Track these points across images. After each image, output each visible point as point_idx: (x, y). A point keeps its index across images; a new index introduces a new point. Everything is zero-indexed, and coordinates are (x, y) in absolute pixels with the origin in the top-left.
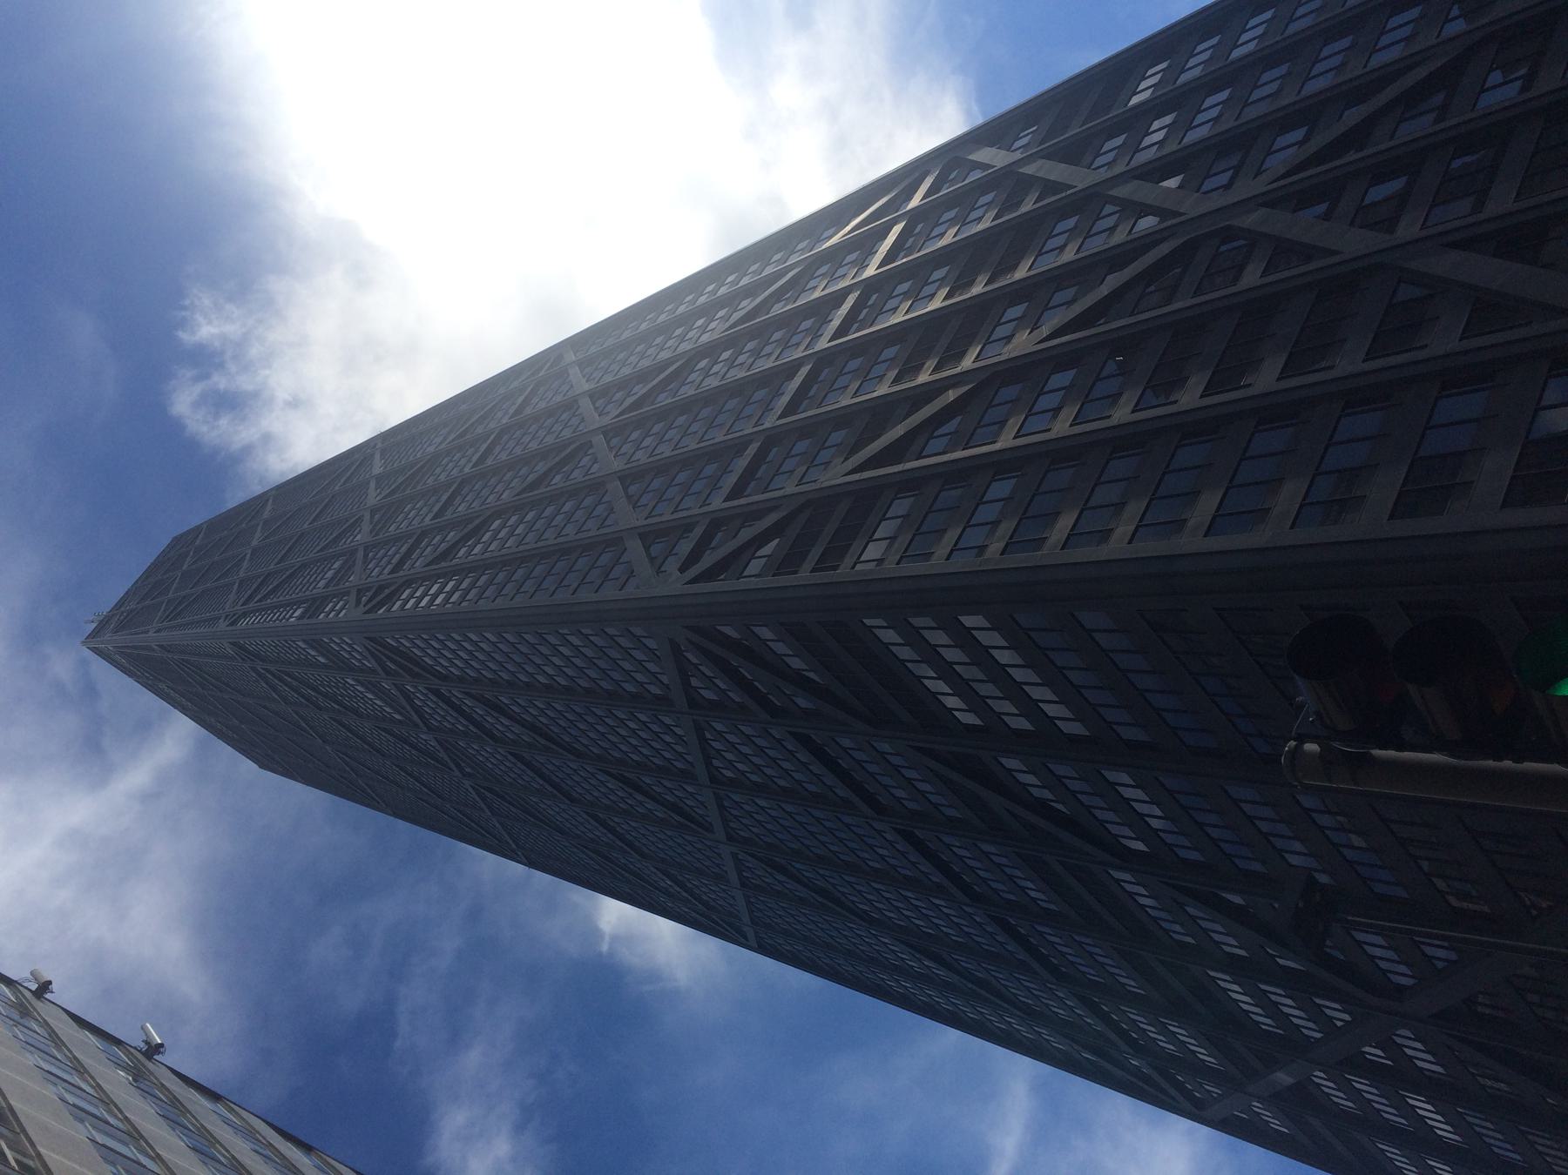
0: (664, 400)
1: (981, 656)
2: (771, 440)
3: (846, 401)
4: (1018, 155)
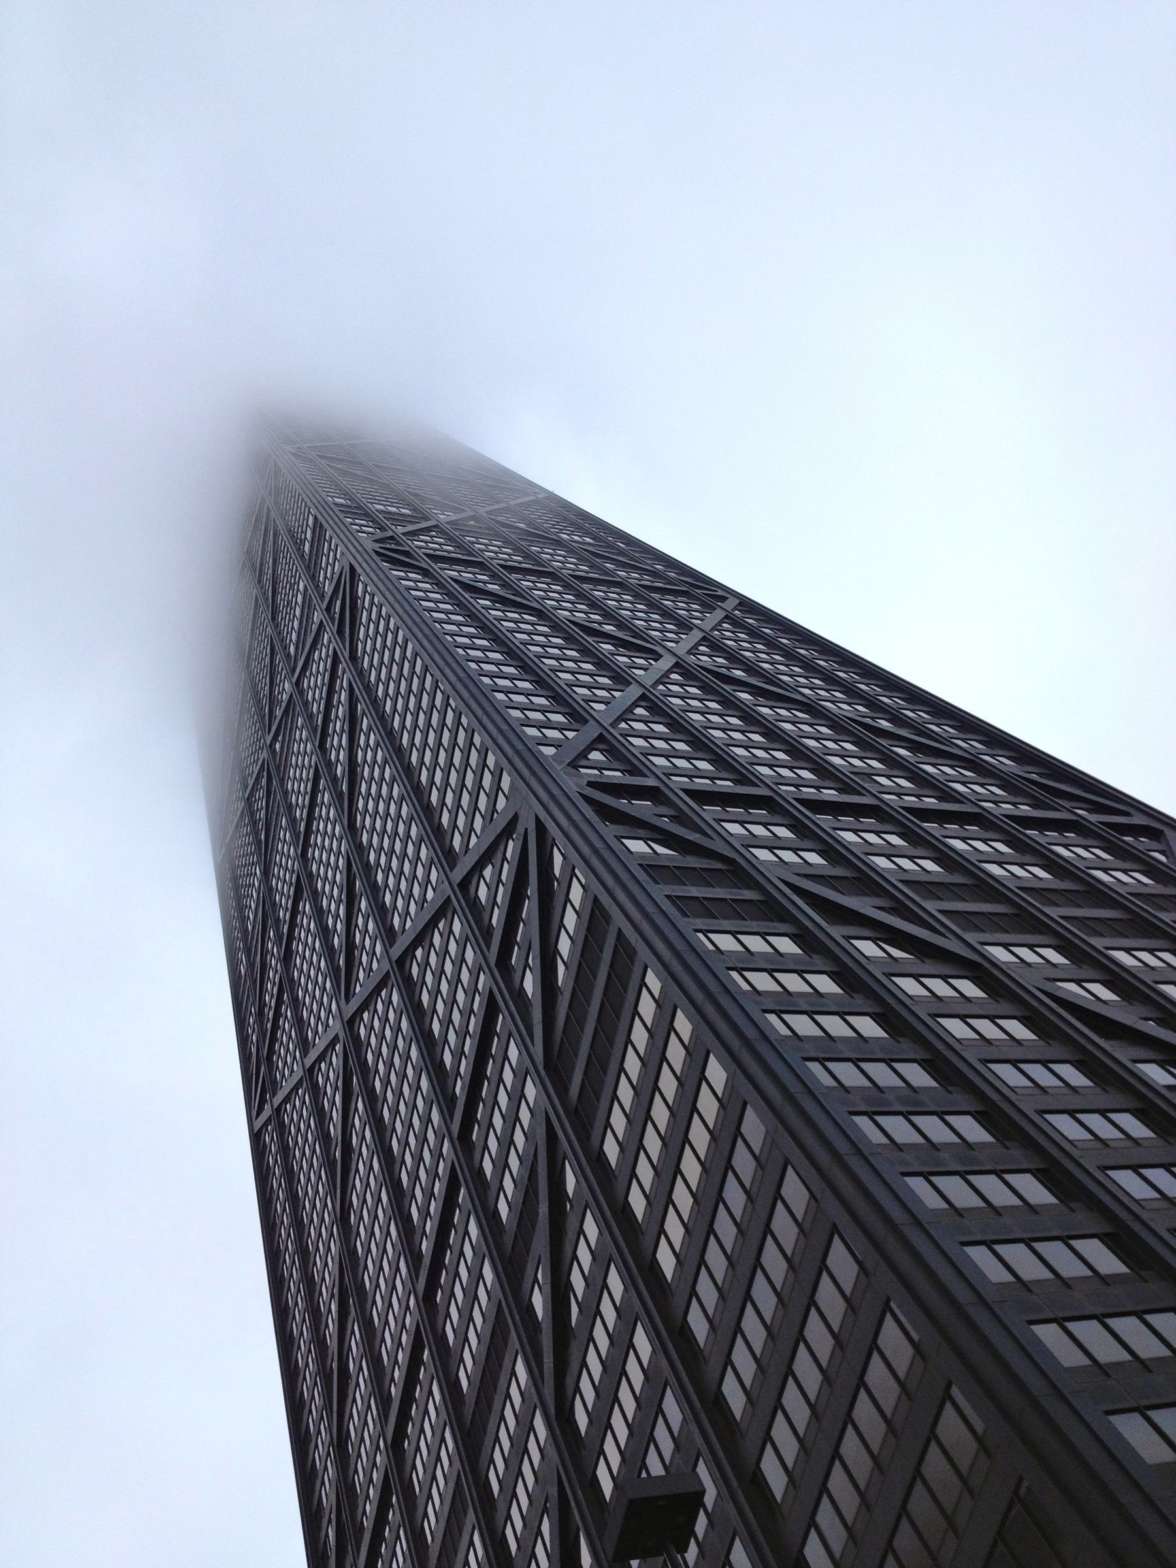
1: (685, 1110)
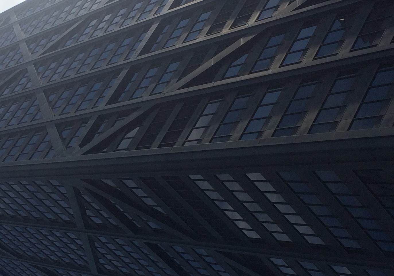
0: (70, 44)
1: (260, 197)
2: (135, 68)
3: (179, 45)
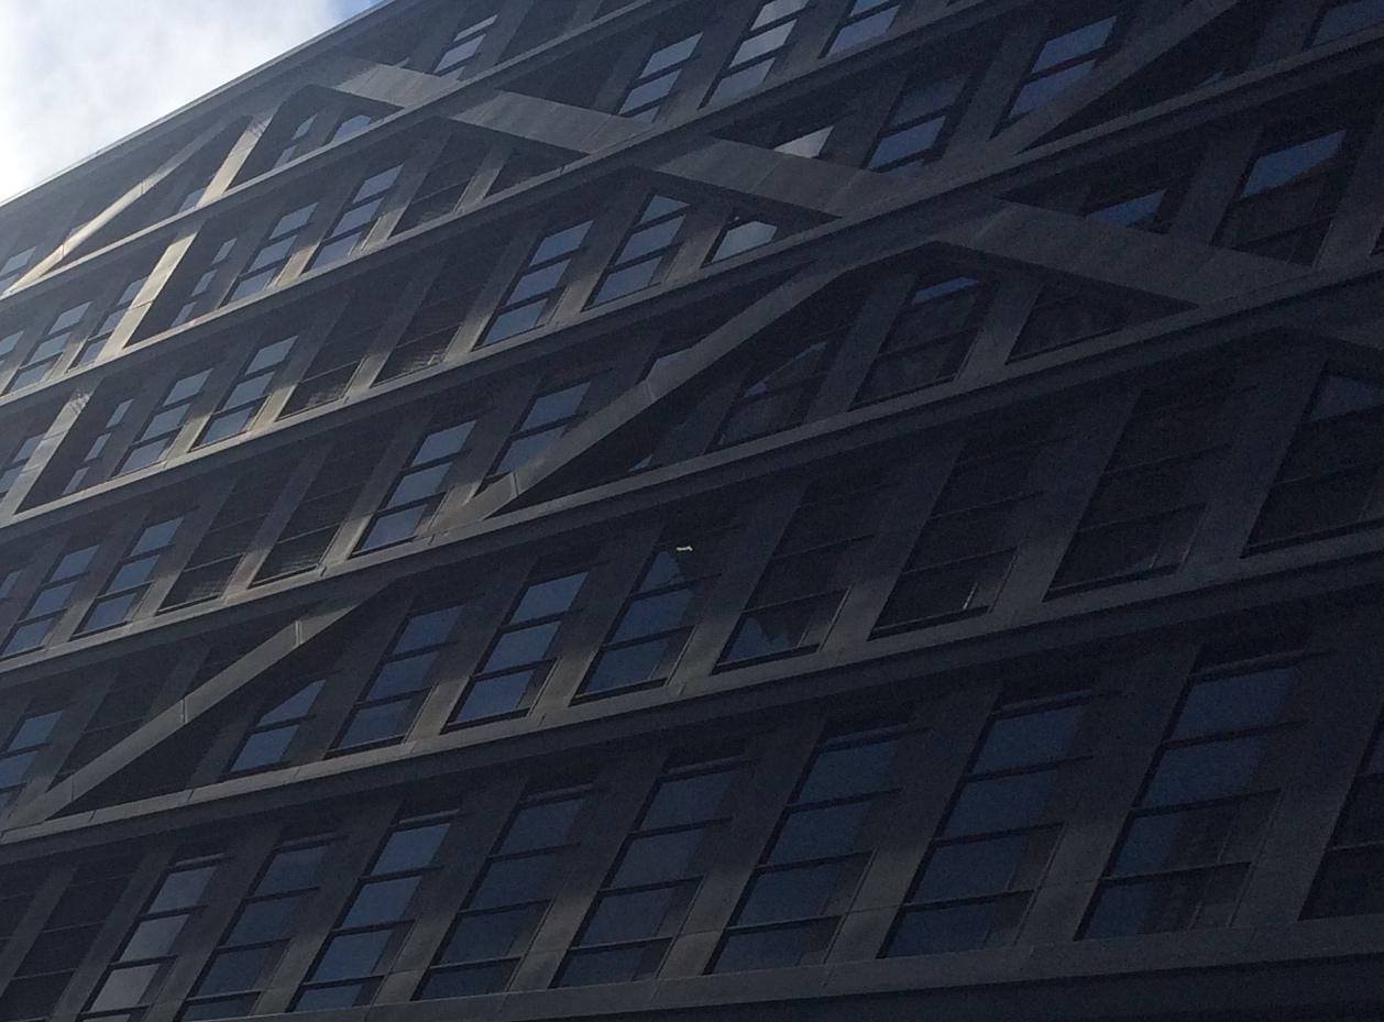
4: (452, 83)
